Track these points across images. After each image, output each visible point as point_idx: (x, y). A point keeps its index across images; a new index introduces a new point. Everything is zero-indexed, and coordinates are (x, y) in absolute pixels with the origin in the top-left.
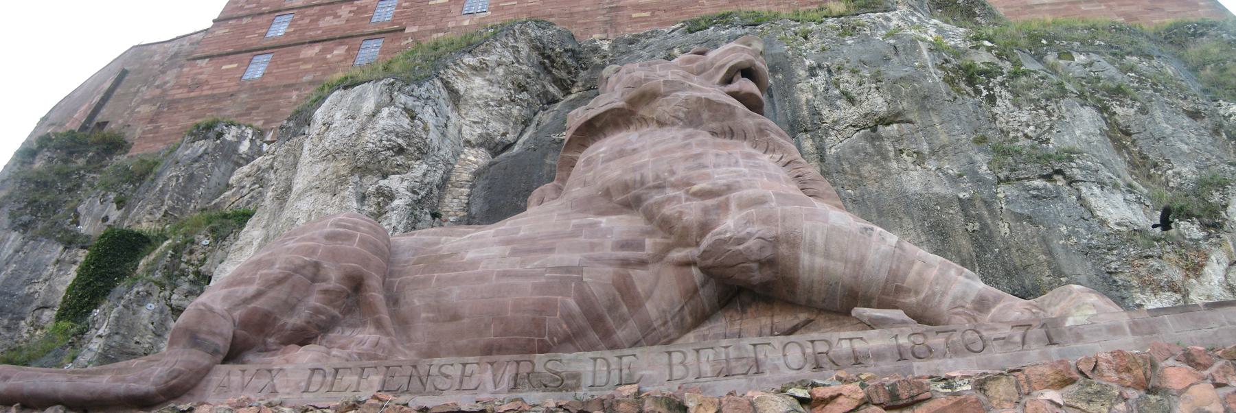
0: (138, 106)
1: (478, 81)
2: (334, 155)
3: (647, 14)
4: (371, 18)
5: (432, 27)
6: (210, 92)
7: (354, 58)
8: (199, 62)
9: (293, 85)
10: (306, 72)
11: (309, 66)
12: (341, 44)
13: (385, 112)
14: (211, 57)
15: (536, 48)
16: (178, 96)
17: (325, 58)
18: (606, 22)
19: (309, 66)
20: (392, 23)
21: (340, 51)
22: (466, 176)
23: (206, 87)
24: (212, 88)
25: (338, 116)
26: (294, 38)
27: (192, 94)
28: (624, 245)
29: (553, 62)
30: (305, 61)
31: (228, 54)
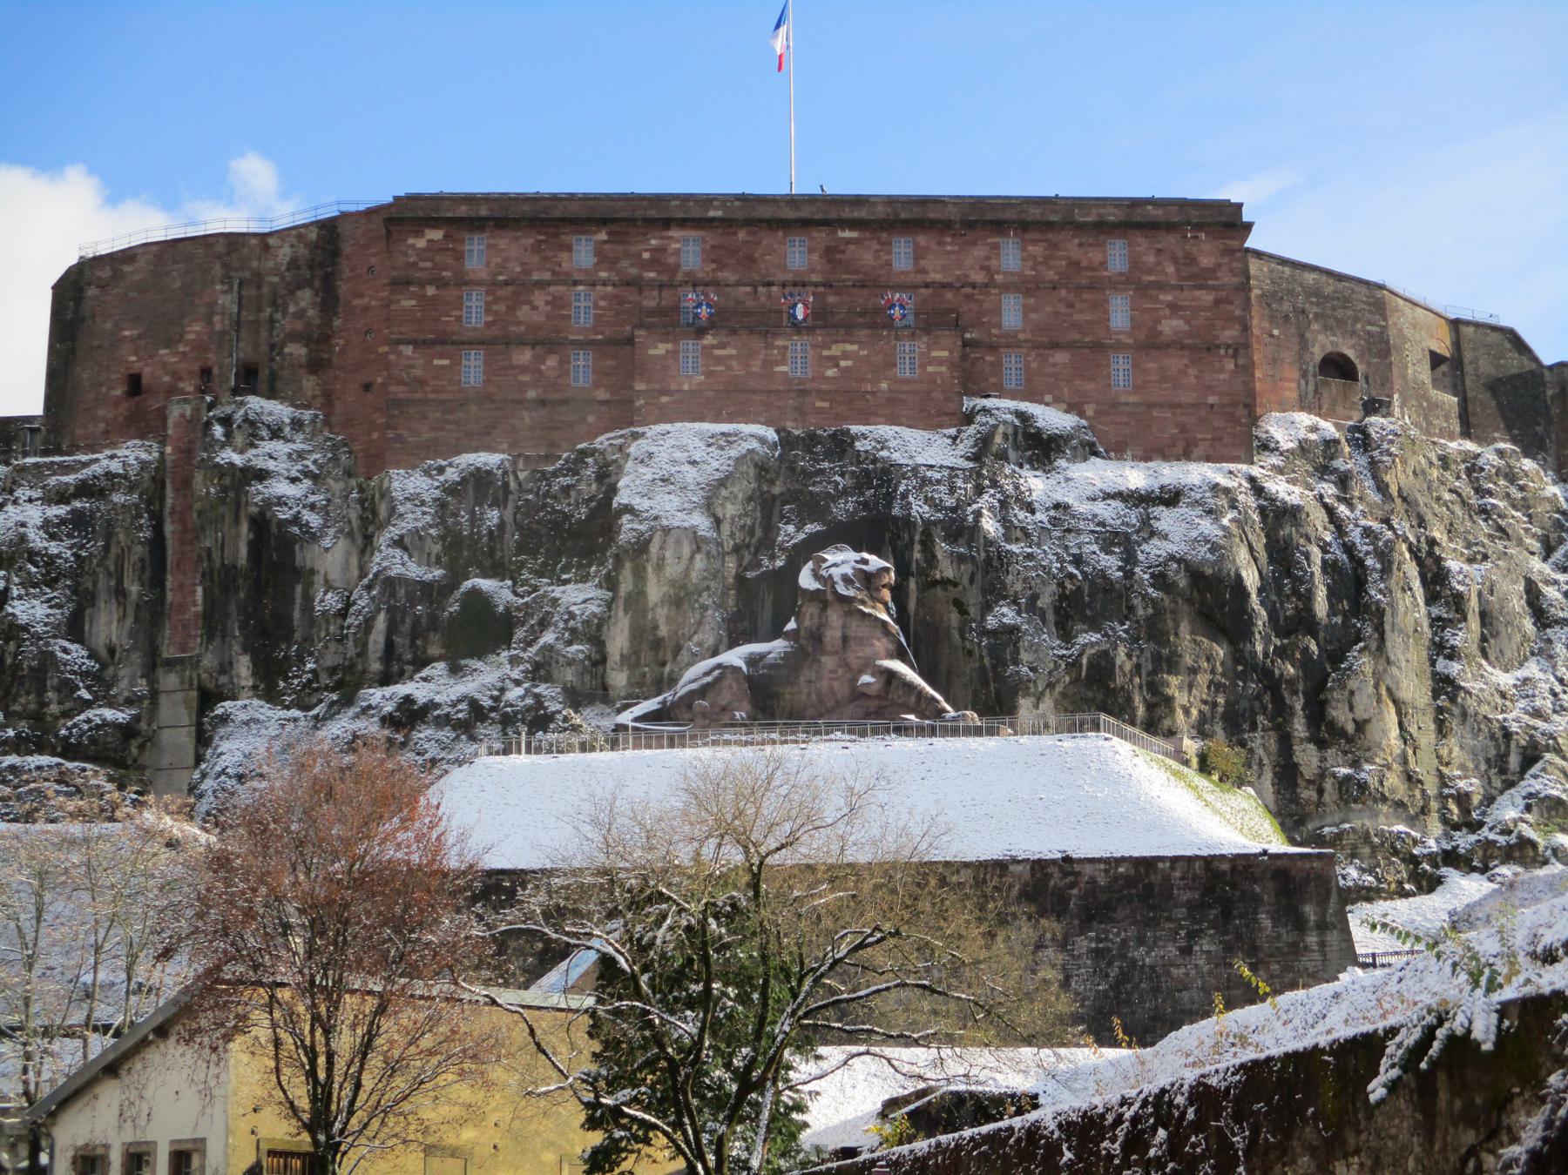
0: (284, 345)
1: (729, 505)
2: (672, 583)
3: (826, 405)
4: (569, 316)
5: (657, 386)
6: (431, 396)
7: (567, 373)
8: (402, 347)
9: (519, 402)
10: (524, 386)
11: (526, 378)
12: (551, 352)
13: (698, 557)
14: (415, 343)
15: (756, 465)
16: (402, 396)
17: (540, 371)
18: (796, 409)
19: (526, 378)
20: (595, 331)
21: (552, 361)
22: (731, 580)
23: (428, 389)
24: (435, 391)
25: (668, 554)
26: (496, 331)
27: (417, 396)
28: (832, 672)
29: (767, 471)
30: (523, 369)
31: (434, 342)
